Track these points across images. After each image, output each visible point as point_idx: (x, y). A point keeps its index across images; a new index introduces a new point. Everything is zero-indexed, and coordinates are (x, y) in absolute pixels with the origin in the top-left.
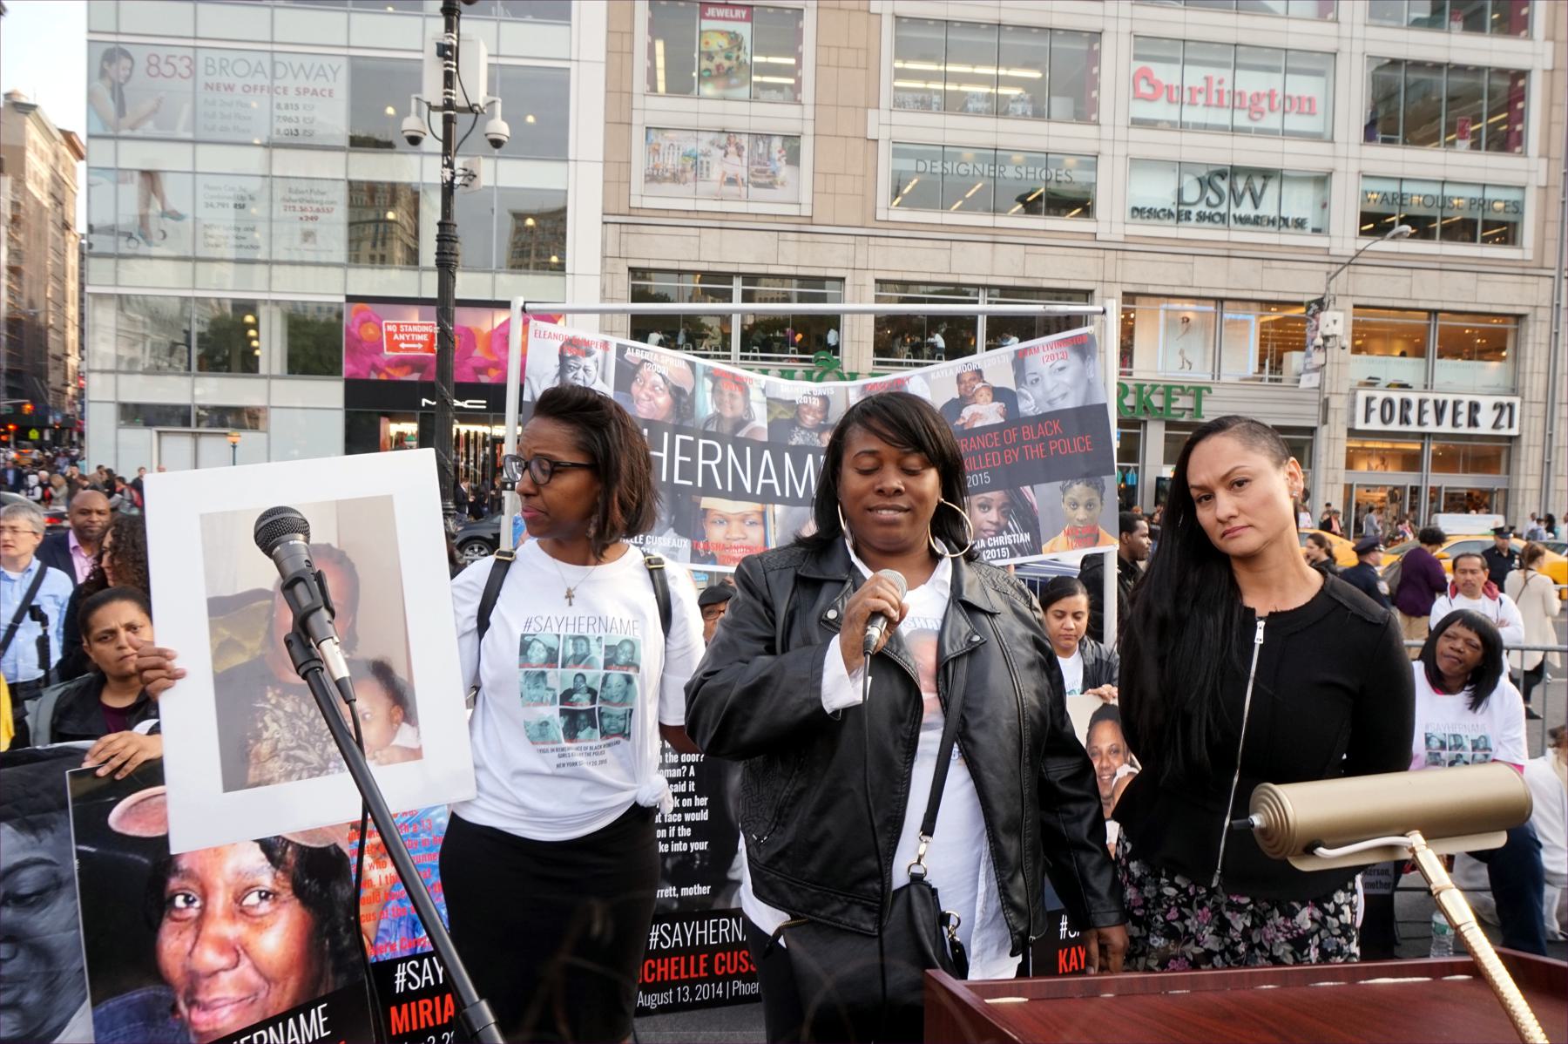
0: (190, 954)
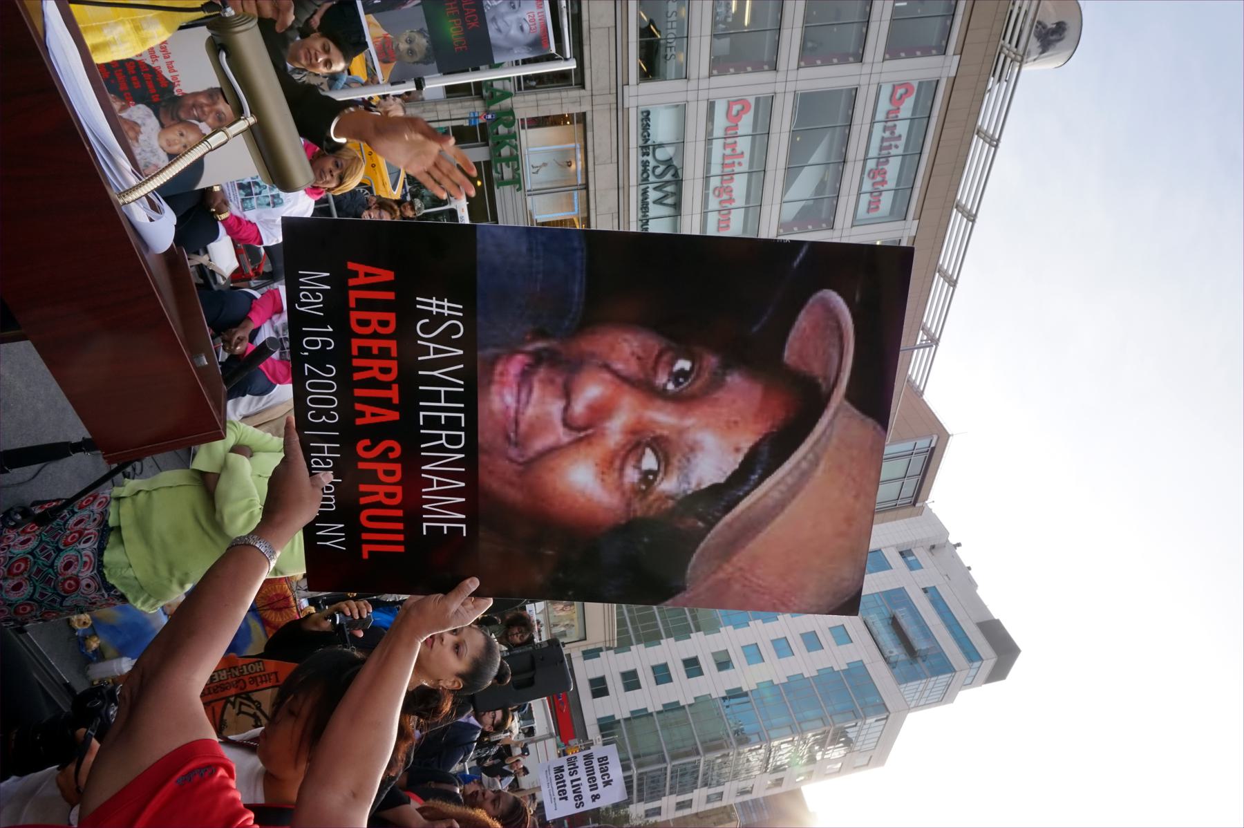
0: (607, 367)
